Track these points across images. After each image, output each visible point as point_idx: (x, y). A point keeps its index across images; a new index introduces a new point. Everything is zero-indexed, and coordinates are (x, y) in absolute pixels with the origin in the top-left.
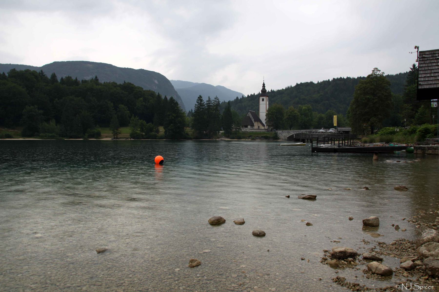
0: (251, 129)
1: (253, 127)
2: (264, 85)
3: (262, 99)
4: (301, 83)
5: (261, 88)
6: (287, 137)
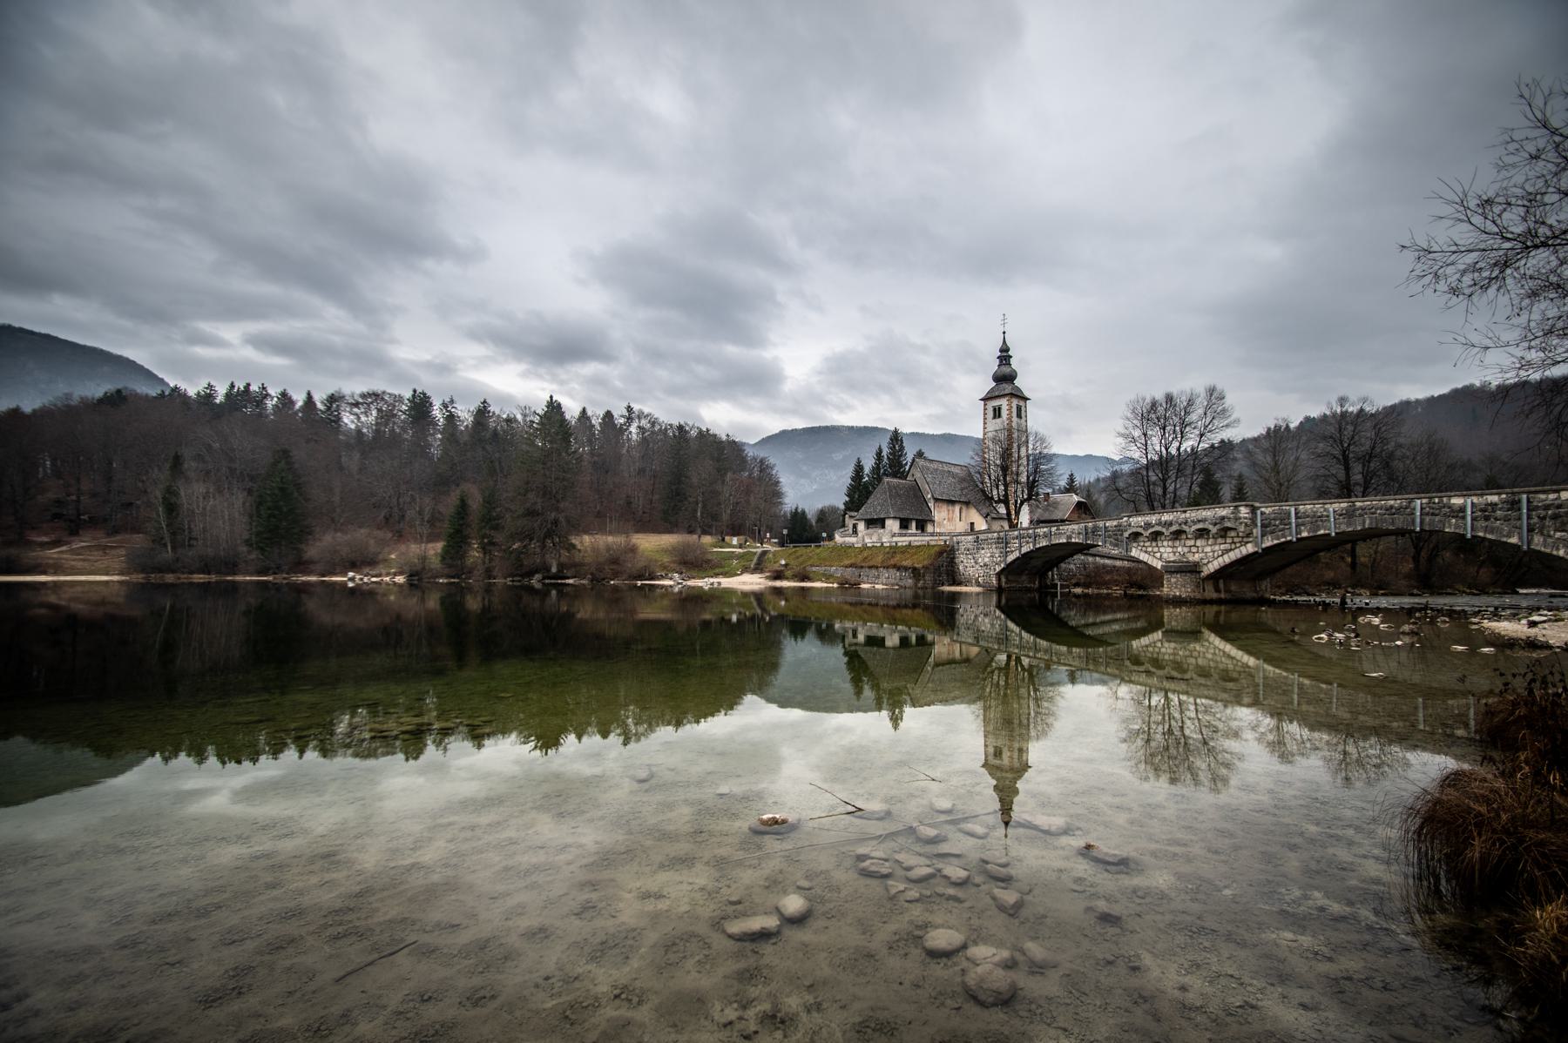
0: (901, 535)
3: (995, 410)
5: (994, 366)
6: (998, 569)
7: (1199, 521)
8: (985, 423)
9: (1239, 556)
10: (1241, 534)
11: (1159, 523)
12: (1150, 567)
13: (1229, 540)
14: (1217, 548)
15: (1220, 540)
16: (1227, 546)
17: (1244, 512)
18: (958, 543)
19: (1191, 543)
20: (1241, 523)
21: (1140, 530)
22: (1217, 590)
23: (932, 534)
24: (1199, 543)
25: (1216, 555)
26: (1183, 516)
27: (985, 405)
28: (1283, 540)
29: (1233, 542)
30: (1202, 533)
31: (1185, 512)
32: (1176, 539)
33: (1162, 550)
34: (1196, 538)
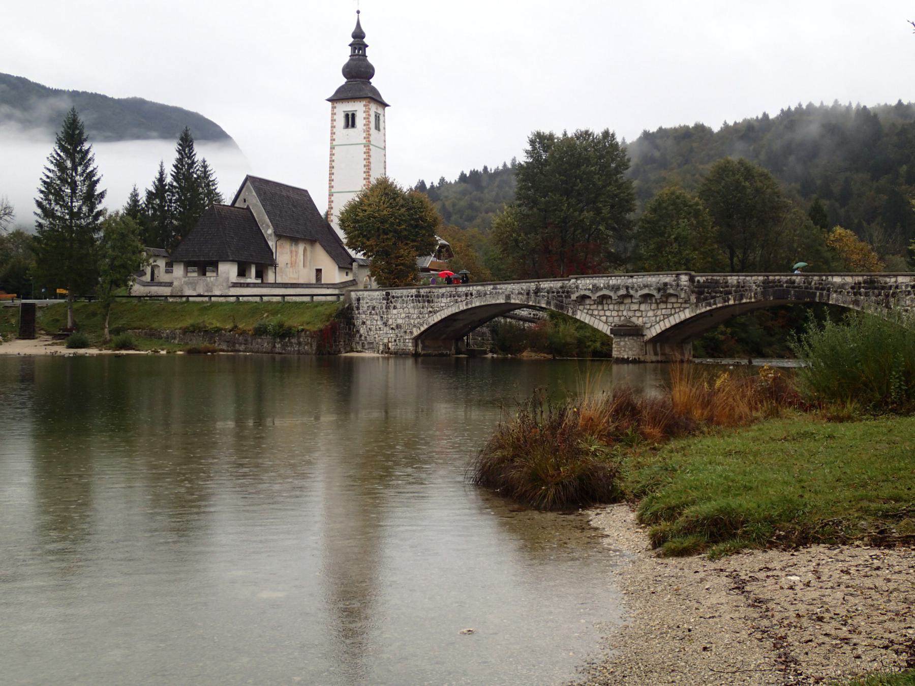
1: (259, 275)
2: (358, 37)
3: (347, 116)
4: (660, 129)
5: (344, 55)
6: (416, 332)
7: (646, 286)
8: (333, 133)
9: (678, 321)
10: (680, 301)
11: (608, 287)
12: (595, 331)
13: (669, 306)
14: (659, 312)
15: (662, 306)
16: (668, 312)
17: (684, 279)
18: (358, 300)
19: (635, 307)
20: (682, 289)
21: (588, 293)
22: (656, 354)
23: (276, 285)
24: (643, 307)
25: (658, 319)
26: (630, 280)
27: (333, 108)
28: (714, 307)
29: (673, 308)
30: (646, 298)
31: (632, 277)
32: (622, 303)
33: (608, 313)
34: (640, 303)
